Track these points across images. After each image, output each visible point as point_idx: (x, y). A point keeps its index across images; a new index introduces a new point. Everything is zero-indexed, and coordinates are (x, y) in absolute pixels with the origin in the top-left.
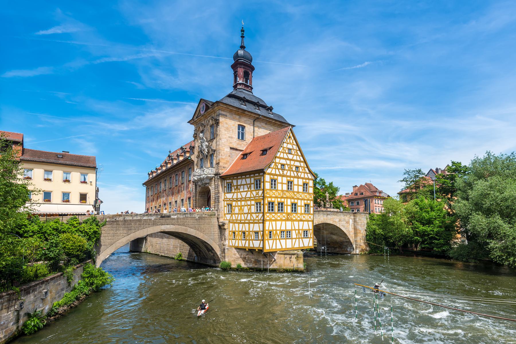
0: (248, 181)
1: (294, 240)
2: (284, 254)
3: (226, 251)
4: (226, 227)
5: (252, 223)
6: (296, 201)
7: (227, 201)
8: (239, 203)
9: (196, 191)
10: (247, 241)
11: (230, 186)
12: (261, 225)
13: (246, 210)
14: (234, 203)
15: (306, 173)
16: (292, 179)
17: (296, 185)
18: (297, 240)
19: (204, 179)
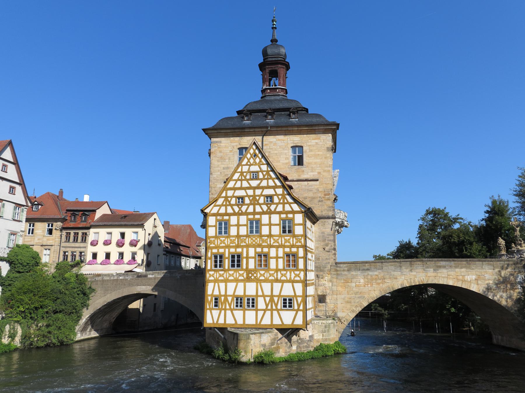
1: (260, 313)
6: (266, 250)
15: (288, 203)
16: (257, 217)
18: (268, 313)
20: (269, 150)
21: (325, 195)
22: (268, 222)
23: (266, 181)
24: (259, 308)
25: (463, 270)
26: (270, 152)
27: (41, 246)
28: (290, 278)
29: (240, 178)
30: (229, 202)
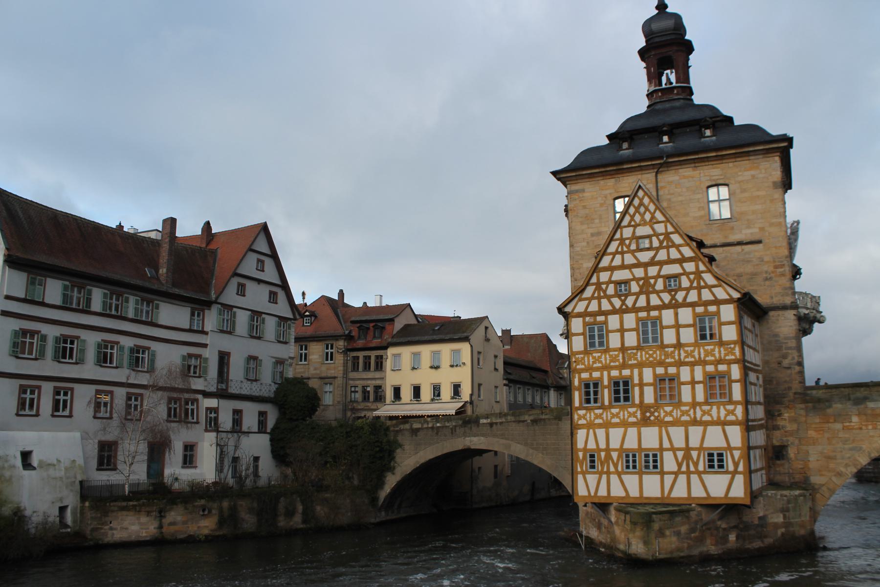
6: (672, 370)
15: (707, 286)
16: (654, 313)
17: (668, 327)
18: (682, 478)
20: (669, 197)
21: (776, 267)
22: (672, 322)
23: (665, 250)
24: (665, 470)
26: (669, 200)
27: (321, 378)
28: (719, 417)
29: (620, 250)
30: (605, 291)
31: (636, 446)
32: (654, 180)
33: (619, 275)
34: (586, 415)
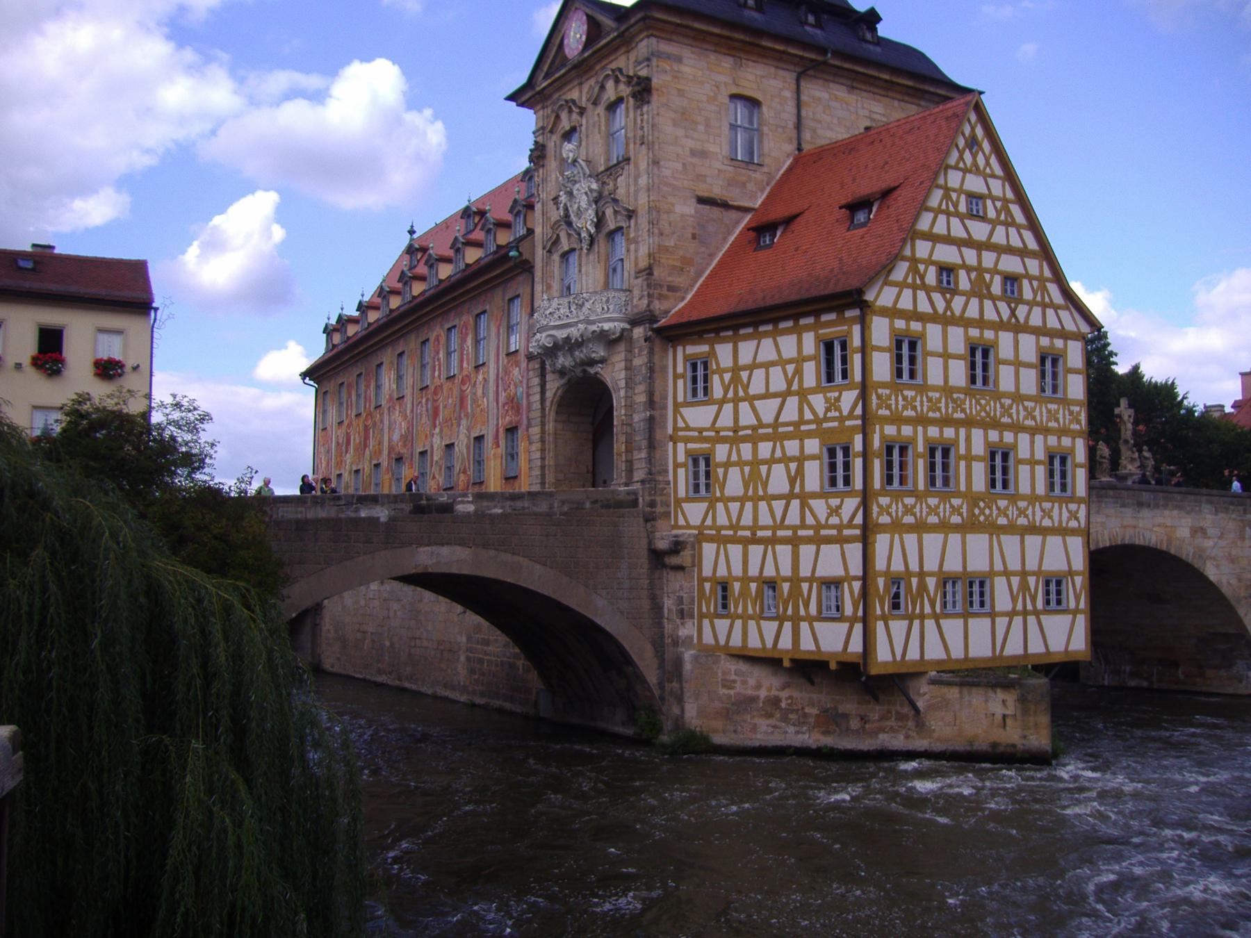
0: (788, 345)
1: (1001, 622)
2: (961, 685)
3: (688, 667)
4: (685, 558)
5: (808, 540)
6: (1008, 437)
7: (687, 440)
8: (746, 449)
9: (543, 400)
10: (788, 626)
11: (700, 372)
12: (854, 551)
13: (778, 480)
14: (721, 452)
16: (989, 334)
17: (1006, 362)
18: (1018, 620)
19: (580, 344)
24: (999, 608)
25: (1175, 512)
26: (814, 131)
28: (1060, 522)
29: (944, 207)
30: (922, 278)
31: (959, 568)
32: (794, 86)
33: (947, 254)
34: (889, 506)
